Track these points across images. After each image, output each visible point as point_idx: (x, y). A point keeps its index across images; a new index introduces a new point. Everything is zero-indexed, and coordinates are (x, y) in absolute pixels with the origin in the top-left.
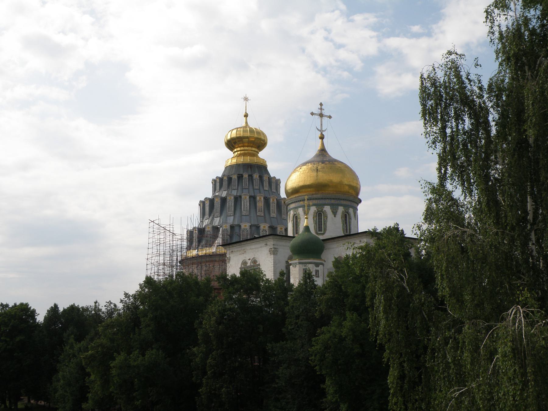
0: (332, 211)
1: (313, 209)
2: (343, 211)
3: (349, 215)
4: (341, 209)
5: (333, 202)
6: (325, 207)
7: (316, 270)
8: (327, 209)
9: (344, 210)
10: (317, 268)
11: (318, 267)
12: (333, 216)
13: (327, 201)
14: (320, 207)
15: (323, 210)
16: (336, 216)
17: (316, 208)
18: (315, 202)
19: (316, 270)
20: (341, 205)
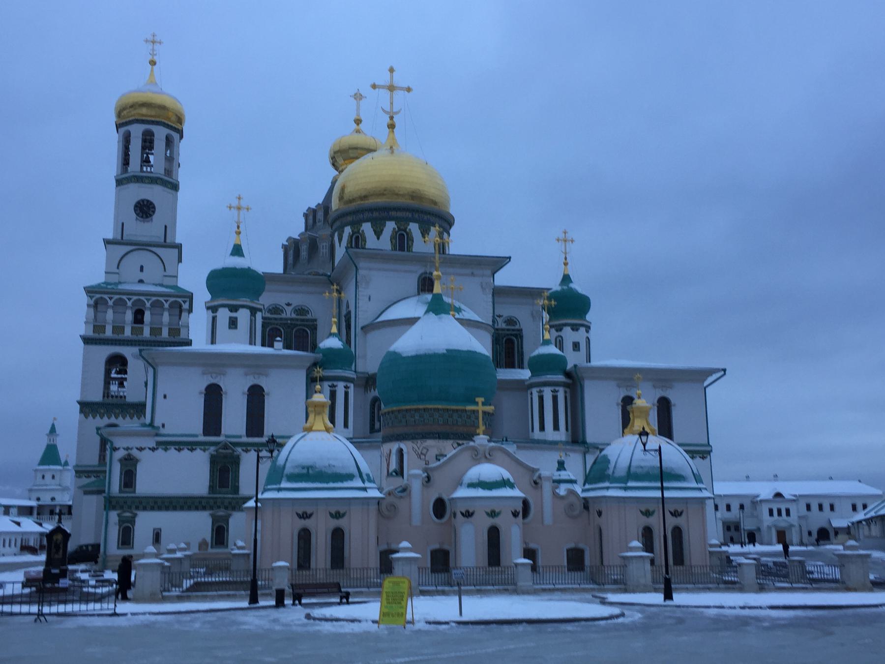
0: (374, 230)
1: (348, 230)
2: (394, 229)
3: (407, 234)
4: (390, 226)
5: (376, 214)
6: (364, 225)
7: (230, 318)
8: (367, 228)
9: (396, 227)
10: (234, 315)
11: (236, 311)
12: (376, 237)
13: (367, 215)
14: (356, 226)
15: (360, 229)
16: (381, 238)
17: (351, 228)
18: (350, 218)
19: (230, 318)
20: (390, 219)
